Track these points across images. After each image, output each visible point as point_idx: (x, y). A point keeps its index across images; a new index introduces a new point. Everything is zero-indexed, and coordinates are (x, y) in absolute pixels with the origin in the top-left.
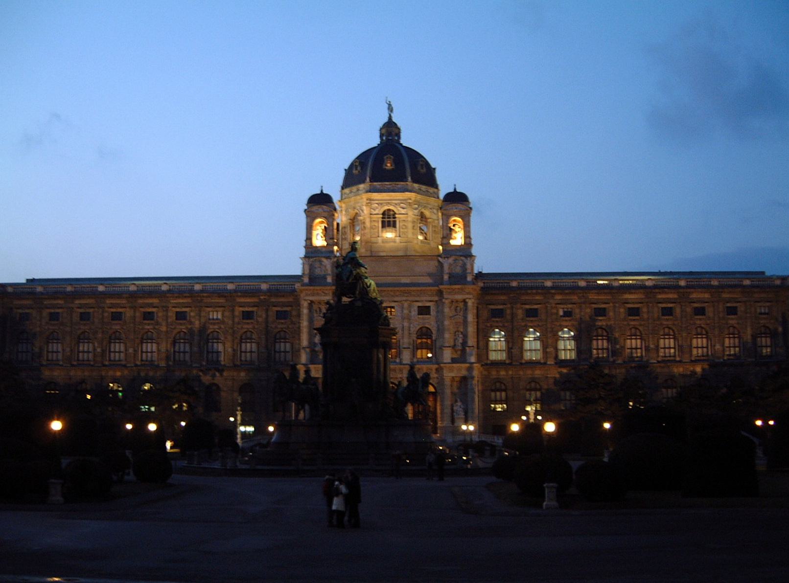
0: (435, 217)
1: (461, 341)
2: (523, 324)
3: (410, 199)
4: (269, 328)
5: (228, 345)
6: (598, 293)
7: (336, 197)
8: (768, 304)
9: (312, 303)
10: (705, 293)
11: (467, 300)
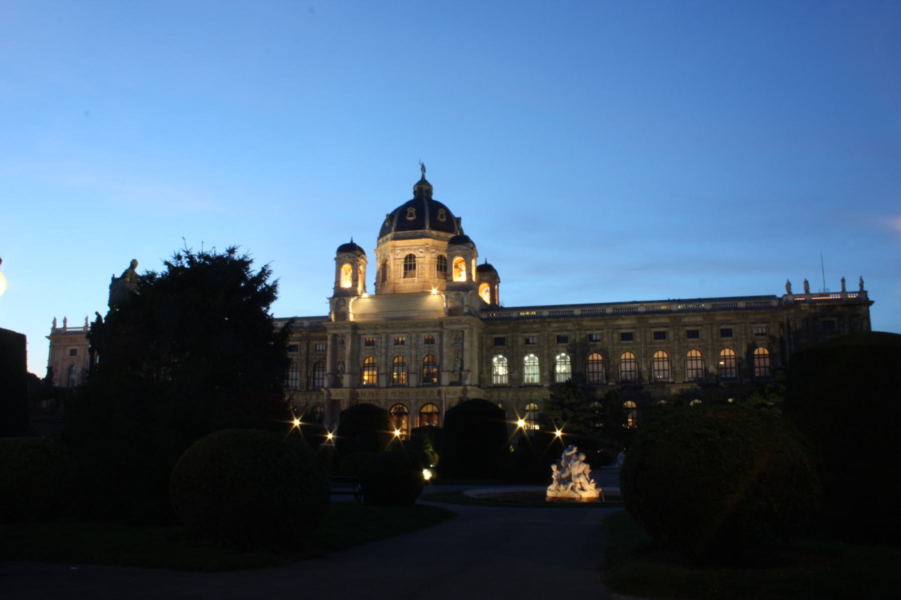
1: (459, 366)
3: (427, 244)
8: (765, 325)
9: (335, 336)
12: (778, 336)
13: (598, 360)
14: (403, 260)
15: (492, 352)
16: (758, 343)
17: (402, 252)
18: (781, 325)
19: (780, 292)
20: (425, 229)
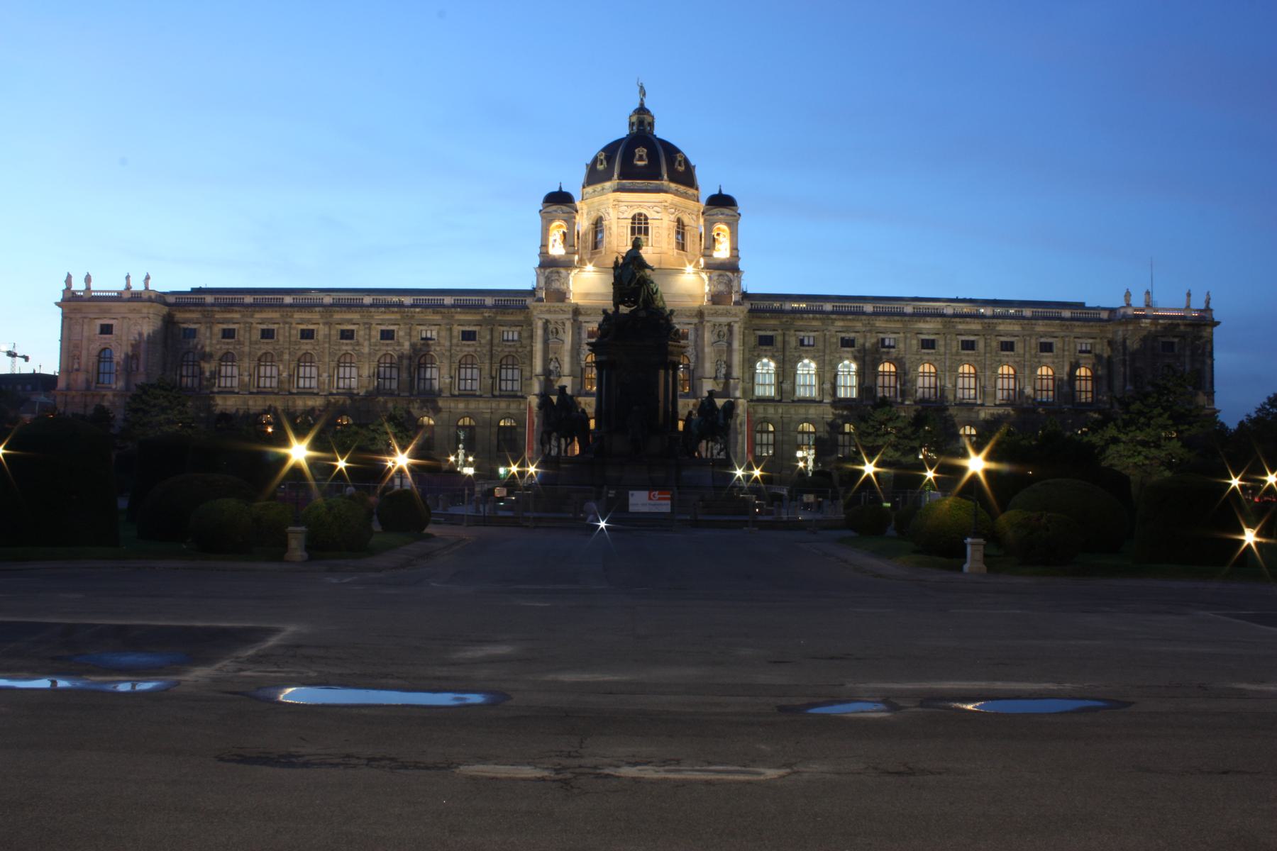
0: (696, 224)
1: (723, 371)
2: (796, 354)
3: (666, 202)
4: (494, 351)
5: (445, 371)
6: (887, 321)
7: (576, 192)
8: (1091, 341)
10: (1014, 324)
11: (732, 324)
12: (1105, 355)
13: (890, 372)
14: (631, 221)
15: (756, 354)
16: (1081, 361)
17: (629, 210)
18: (1110, 343)
19: (1117, 302)
20: (662, 180)
